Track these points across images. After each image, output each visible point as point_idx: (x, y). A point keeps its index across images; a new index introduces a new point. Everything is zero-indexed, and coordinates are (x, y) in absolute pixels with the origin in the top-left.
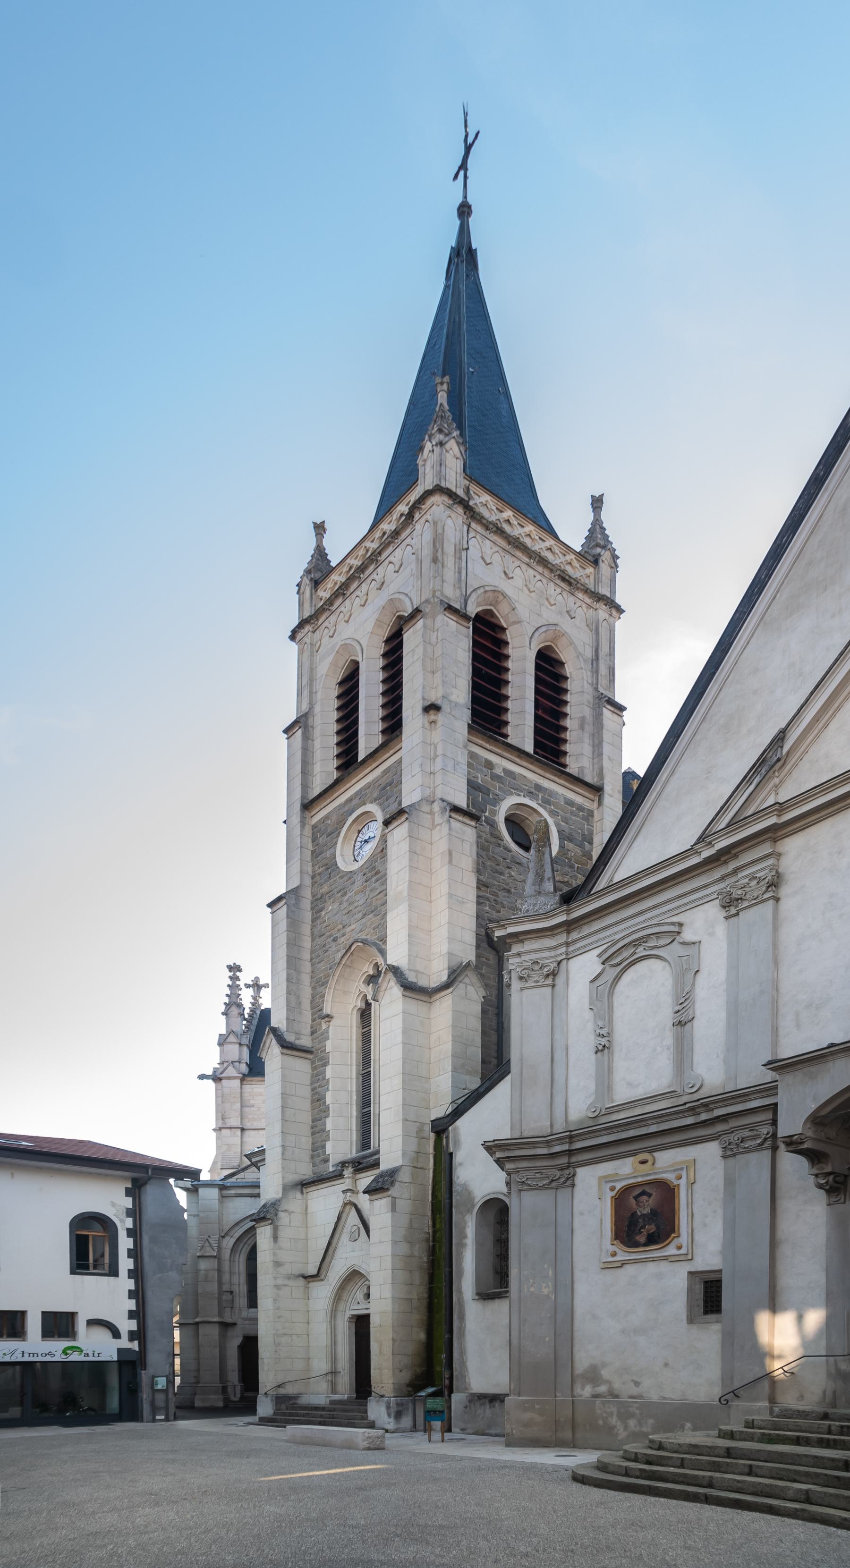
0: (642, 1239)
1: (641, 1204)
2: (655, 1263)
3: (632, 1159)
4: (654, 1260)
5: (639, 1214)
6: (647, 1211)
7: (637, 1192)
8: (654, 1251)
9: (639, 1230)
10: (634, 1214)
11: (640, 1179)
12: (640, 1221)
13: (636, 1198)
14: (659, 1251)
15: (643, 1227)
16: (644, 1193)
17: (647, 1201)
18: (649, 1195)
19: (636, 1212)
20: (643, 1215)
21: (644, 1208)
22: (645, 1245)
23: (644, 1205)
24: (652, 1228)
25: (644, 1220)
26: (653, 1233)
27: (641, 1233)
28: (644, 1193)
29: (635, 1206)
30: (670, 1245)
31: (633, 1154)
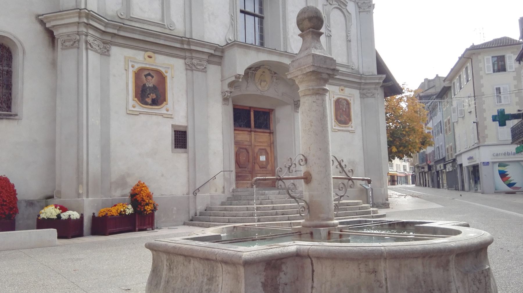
0: (149, 100)
1: (148, 81)
2: (156, 116)
3: (143, 52)
4: (156, 114)
5: (147, 86)
6: (151, 85)
7: (146, 72)
8: (155, 109)
9: (148, 95)
10: (144, 85)
11: (148, 66)
12: (148, 90)
13: (146, 76)
14: (158, 110)
15: (150, 94)
16: (149, 74)
17: (151, 80)
18: (153, 77)
19: (145, 84)
20: (149, 87)
21: (150, 83)
22: (151, 105)
23: (150, 81)
24: (154, 96)
25: (150, 90)
26: (155, 99)
27: (148, 97)
28: (149, 74)
29: (145, 82)
30: (164, 108)
31: (146, 50)
